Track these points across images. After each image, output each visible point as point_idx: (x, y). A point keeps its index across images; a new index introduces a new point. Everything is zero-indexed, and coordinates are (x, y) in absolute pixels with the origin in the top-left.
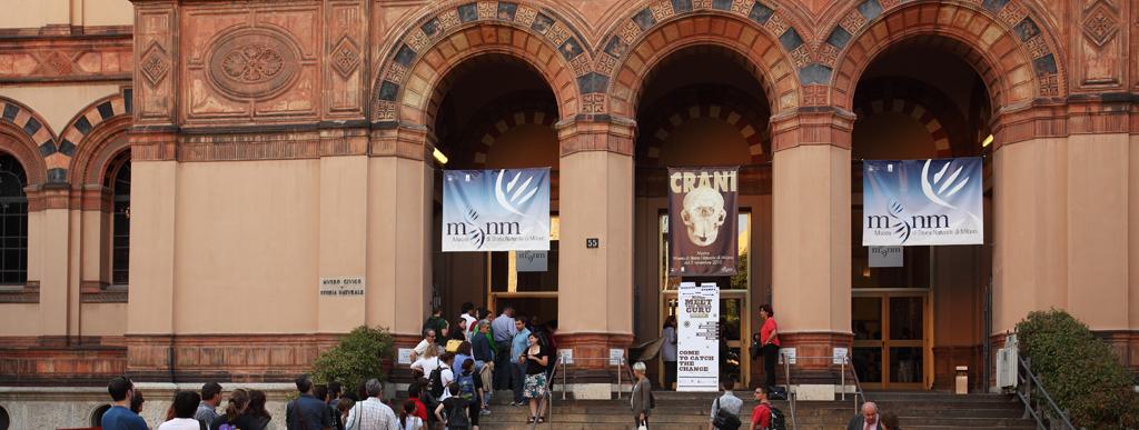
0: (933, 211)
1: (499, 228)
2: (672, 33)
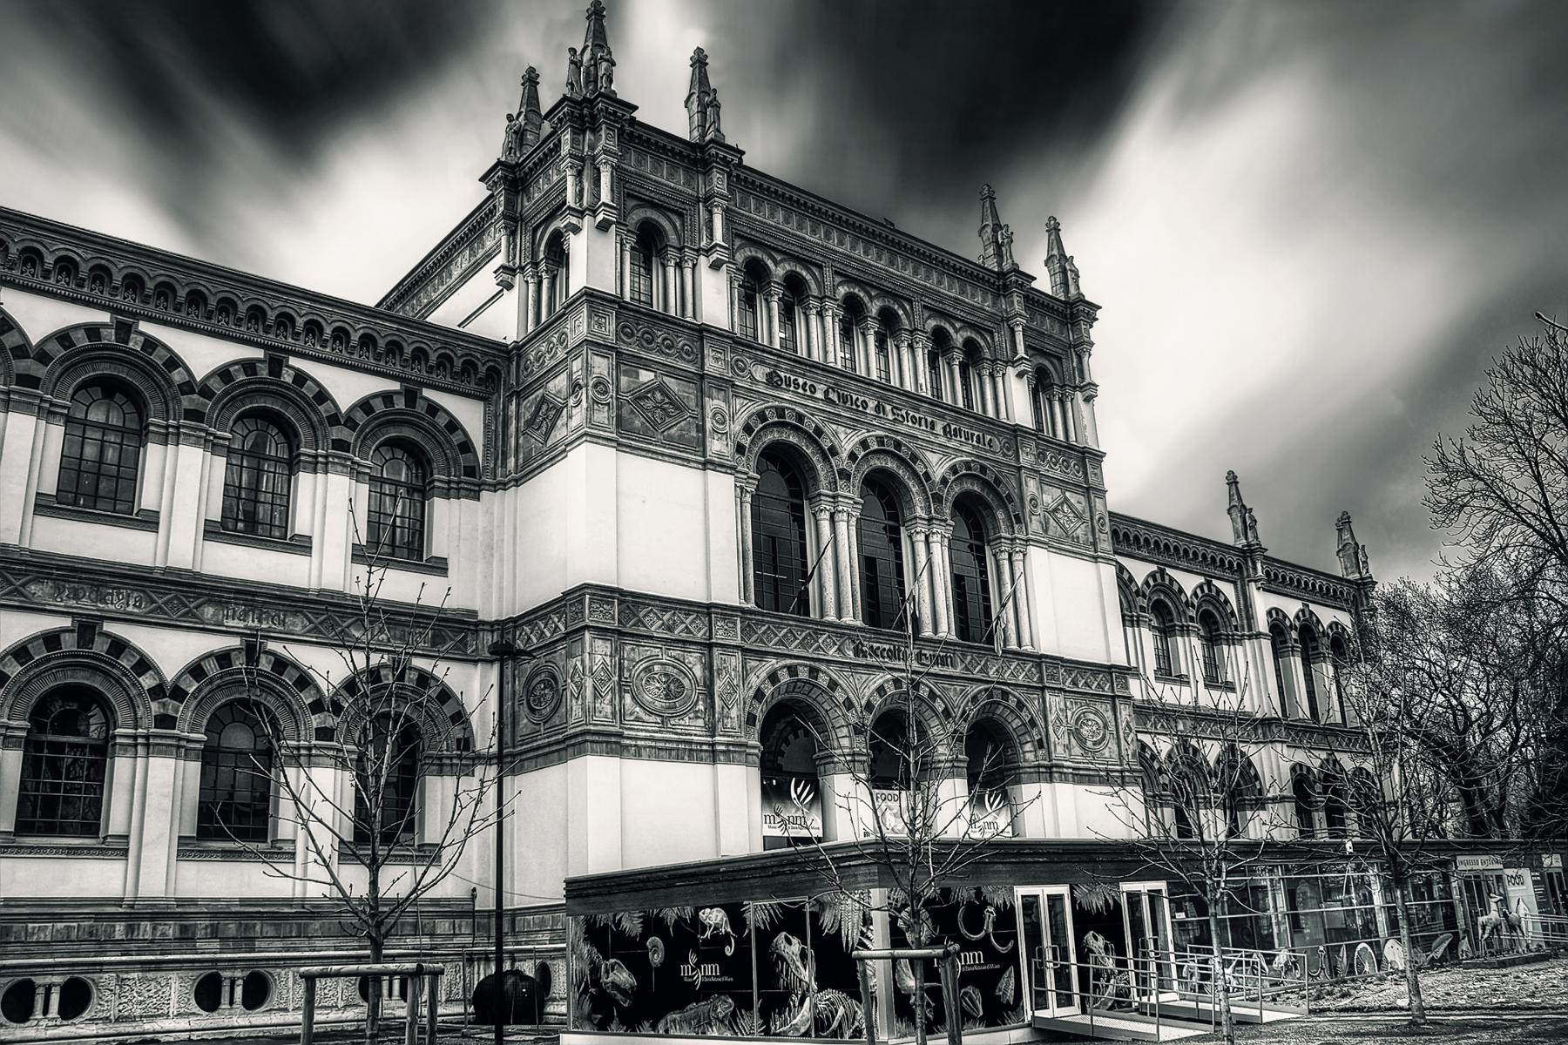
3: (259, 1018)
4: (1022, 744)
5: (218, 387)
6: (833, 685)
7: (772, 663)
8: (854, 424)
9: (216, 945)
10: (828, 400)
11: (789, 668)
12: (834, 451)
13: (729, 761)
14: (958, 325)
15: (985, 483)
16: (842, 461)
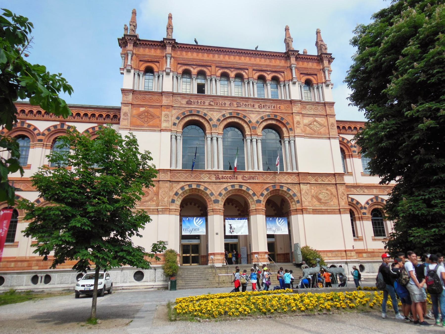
0: (280, 228)
1: (195, 230)
2: (231, 192)
3: (47, 286)
4: (291, 202)
5: (46, 133)
6: (206, 188)
7: (182, 184)
8: (220, 110)
9: (37, 268)
10: (210, 105)
11: (189, 185)
12: (211, 120)
13: (163, 214)
14: (269, 73)
15: (277, 120)
16: (215, 121)
